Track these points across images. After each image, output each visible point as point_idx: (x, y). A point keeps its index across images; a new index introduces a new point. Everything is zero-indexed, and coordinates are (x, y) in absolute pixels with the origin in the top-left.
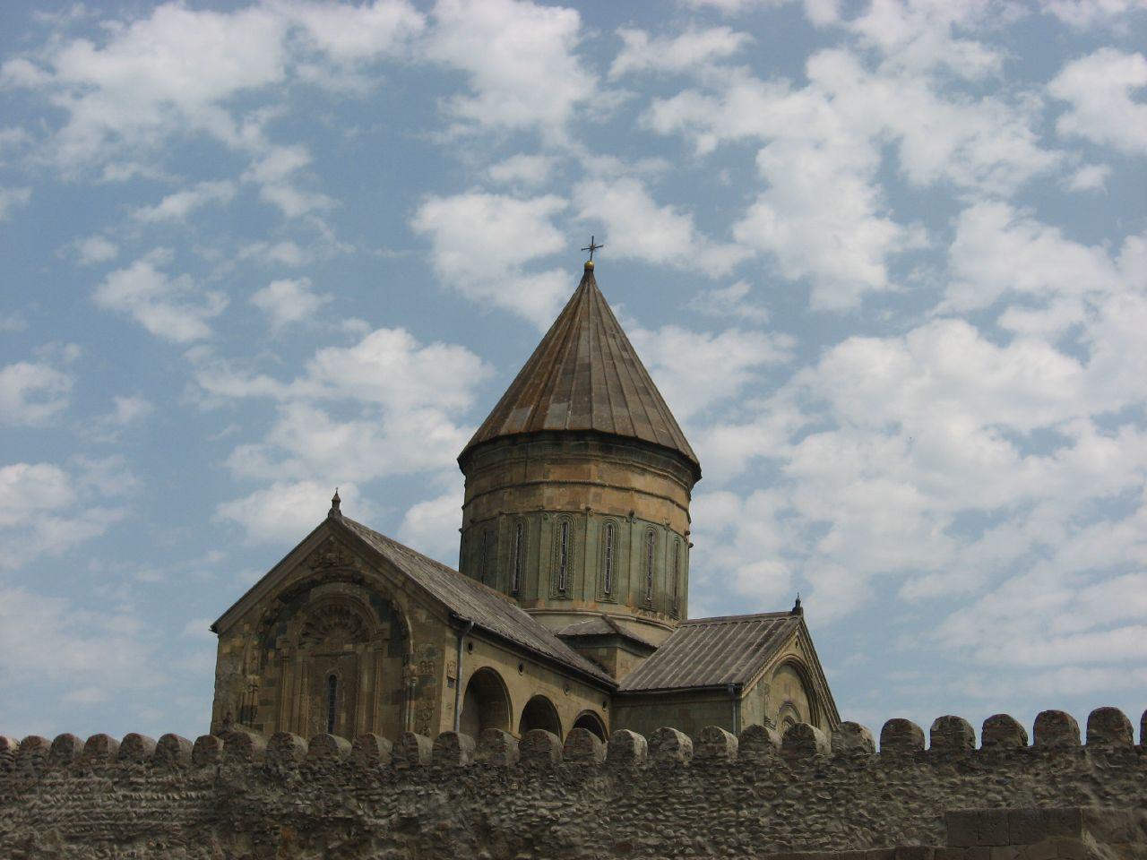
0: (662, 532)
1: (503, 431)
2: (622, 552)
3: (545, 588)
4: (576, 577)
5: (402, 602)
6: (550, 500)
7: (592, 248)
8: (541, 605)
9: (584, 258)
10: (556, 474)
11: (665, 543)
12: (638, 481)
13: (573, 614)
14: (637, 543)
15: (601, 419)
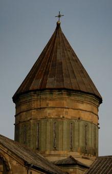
0: (90, 125)
1: (31, 88)
2: (76, 133)
3: (48, 146)
4: (60, 142)
5: (7, 158)
6: (49, 114)
7: (59, 16)
8: (47, 153)
9: (57, 20)
10: (51, 104)
11: (90, 129)
12: (82, 106)
13: (59, 155)
14: (81, 129)
15: (66, 84)
